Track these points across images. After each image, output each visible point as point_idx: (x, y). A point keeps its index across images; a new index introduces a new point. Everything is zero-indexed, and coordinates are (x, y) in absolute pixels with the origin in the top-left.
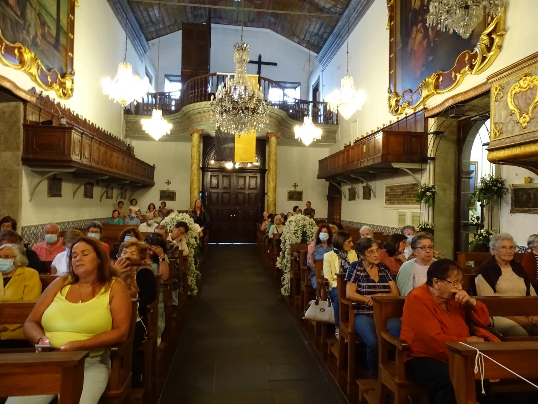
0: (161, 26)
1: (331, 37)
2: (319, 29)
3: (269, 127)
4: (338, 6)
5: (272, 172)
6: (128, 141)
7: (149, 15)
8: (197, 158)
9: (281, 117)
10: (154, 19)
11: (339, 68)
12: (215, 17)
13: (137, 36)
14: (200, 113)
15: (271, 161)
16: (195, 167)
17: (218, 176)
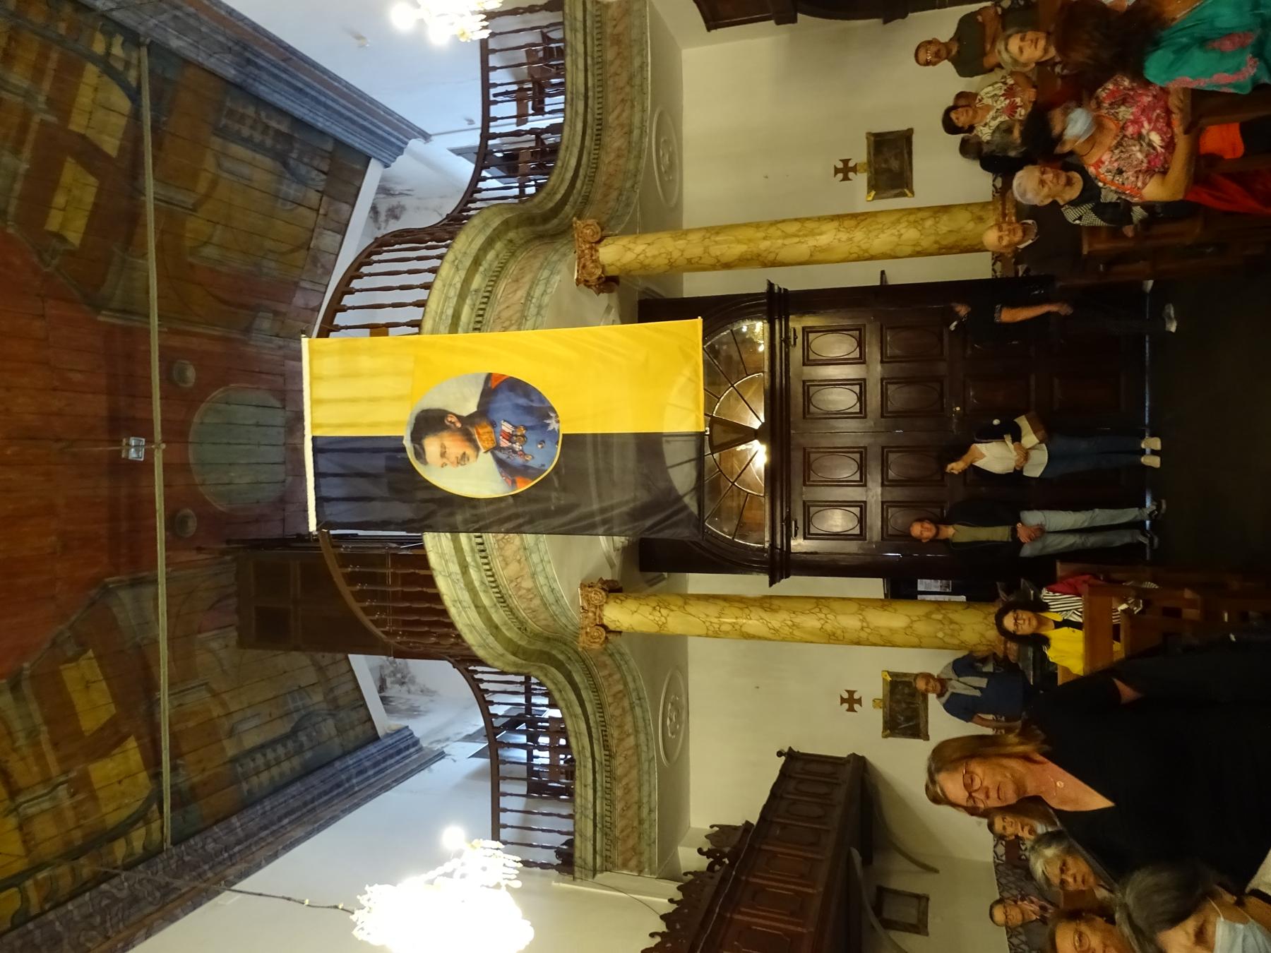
0: (318, 697)
1: (263, 91)
2: (247, 142)
3: (546, 273)
4: (99, 47)
5: (764, 245)
6: (690, 858)
7: (262, 748)
8: (712, 610)
9: (506, 225)
10: (283, 728)
11: (359, 37)
12: (283, 520)
13: (338, 786)
14: (502, 599)
15: (716, 251)
16: (754, 622)
17: (806, 506)
